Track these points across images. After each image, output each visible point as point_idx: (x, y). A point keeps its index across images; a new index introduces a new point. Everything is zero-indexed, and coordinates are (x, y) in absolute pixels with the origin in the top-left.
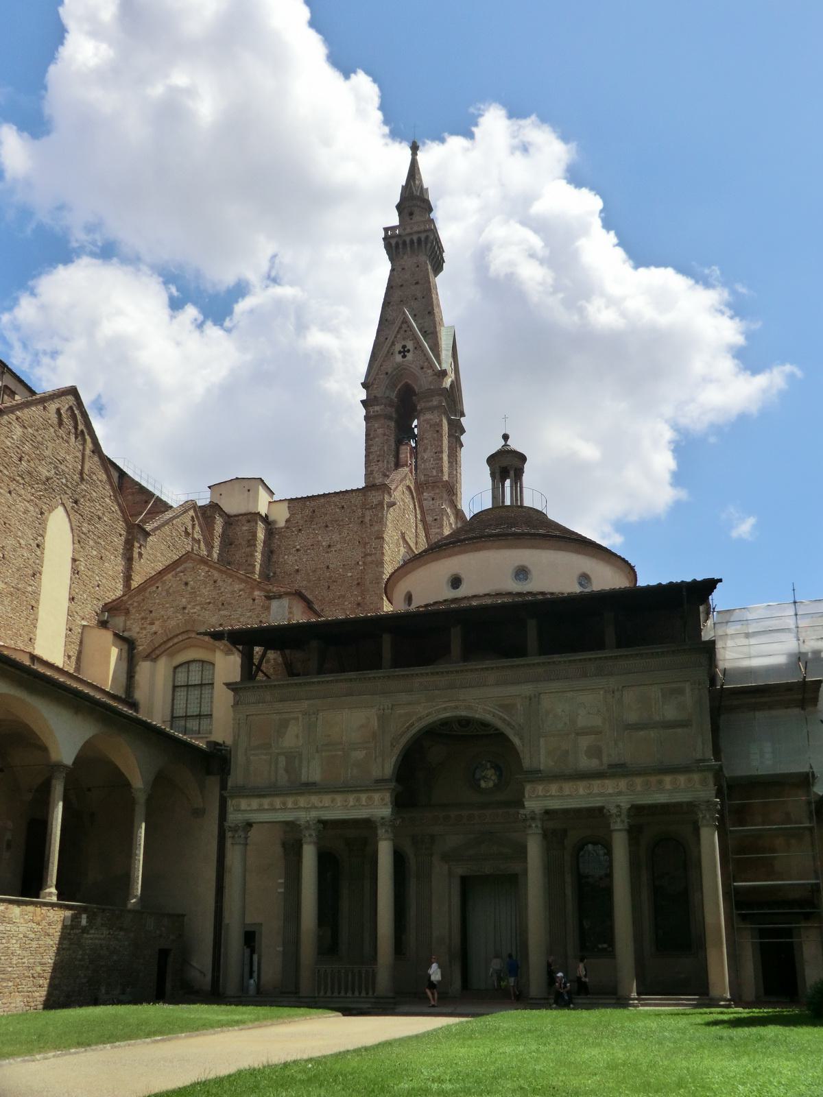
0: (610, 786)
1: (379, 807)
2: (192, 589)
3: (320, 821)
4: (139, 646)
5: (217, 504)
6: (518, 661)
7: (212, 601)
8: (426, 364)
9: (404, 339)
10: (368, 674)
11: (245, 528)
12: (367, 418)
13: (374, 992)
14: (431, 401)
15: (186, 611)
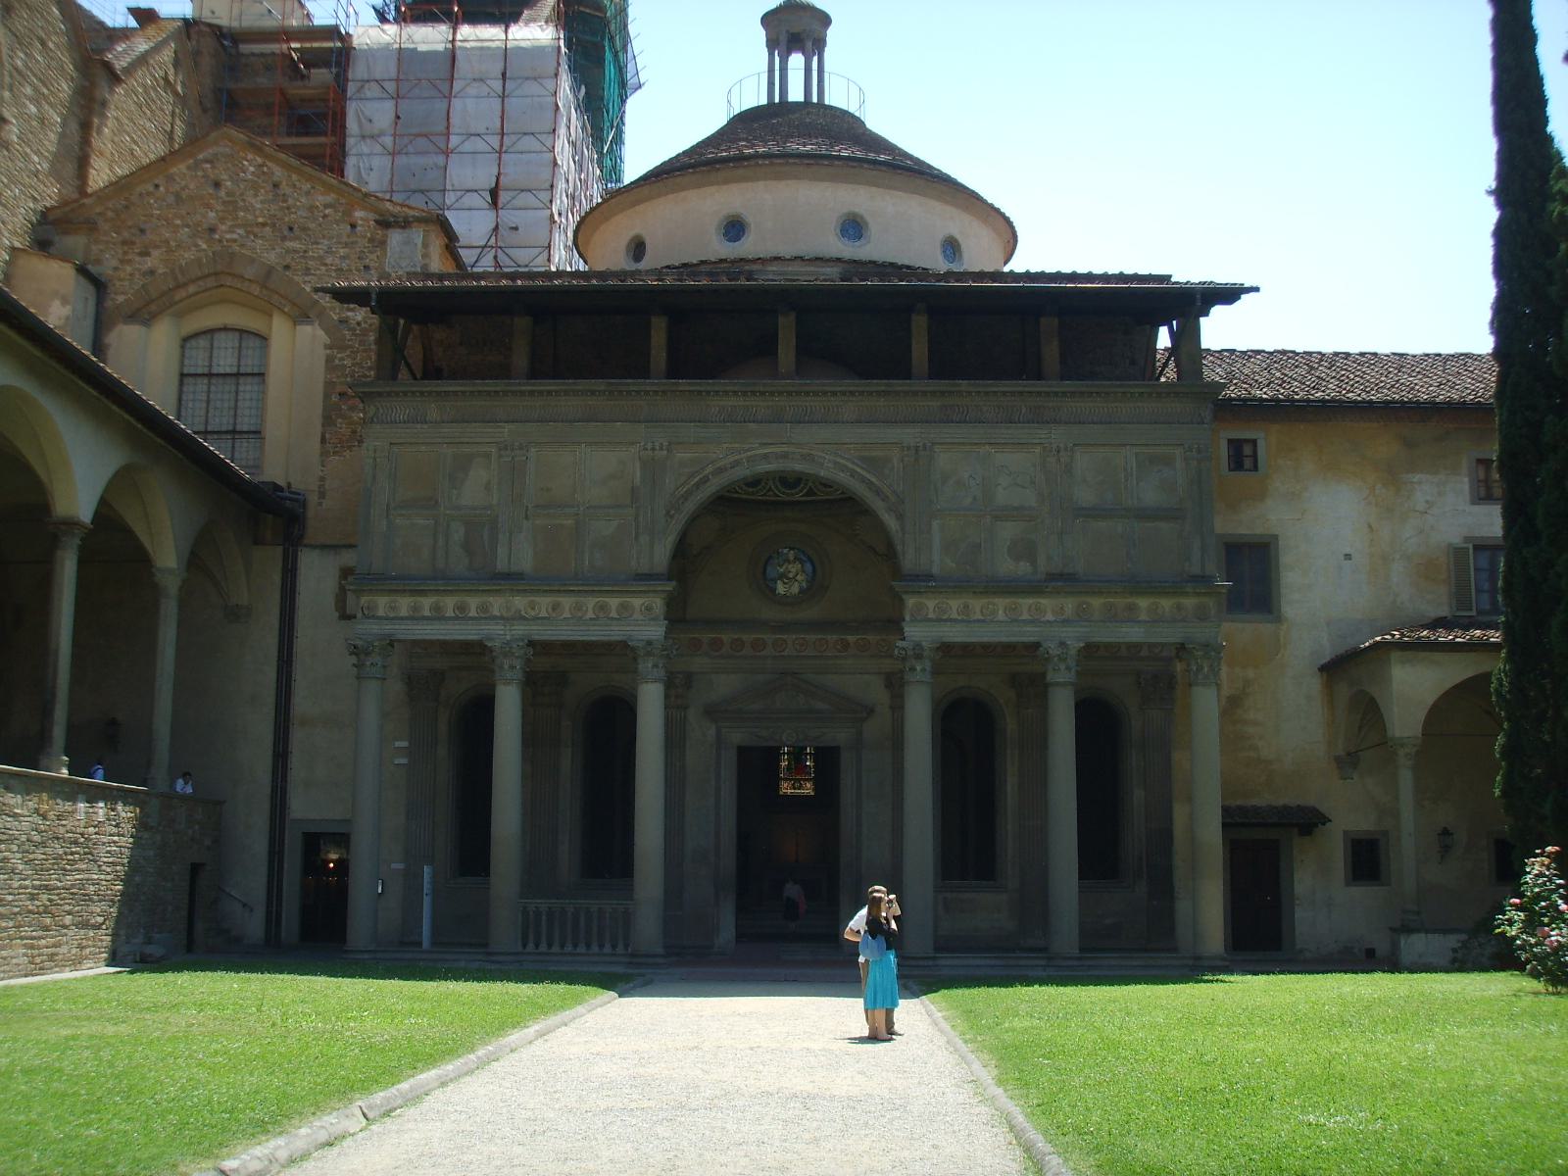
2: (228, 195)
3: (531, 643)
4: (116, 294)
6: (898, 385)
7: (269, 222)
10: (628, 384)
13: (626, 946)
15: (217, 237)
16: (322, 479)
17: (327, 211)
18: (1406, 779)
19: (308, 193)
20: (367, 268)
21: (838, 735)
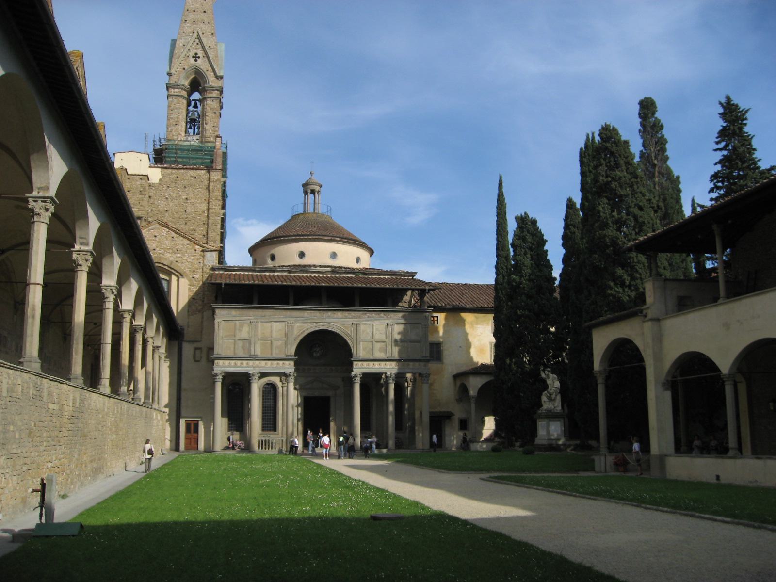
1: (289, 367)
5: (126, 169)
8: (210, 68)
9: (196, 49)
14: (212, 93)
15: (156, 251)
16: (188, 322)
17: (188, 246)
18: (473, 406)
19: (182, 240)
20: (200, 262)
21: (330, 393)
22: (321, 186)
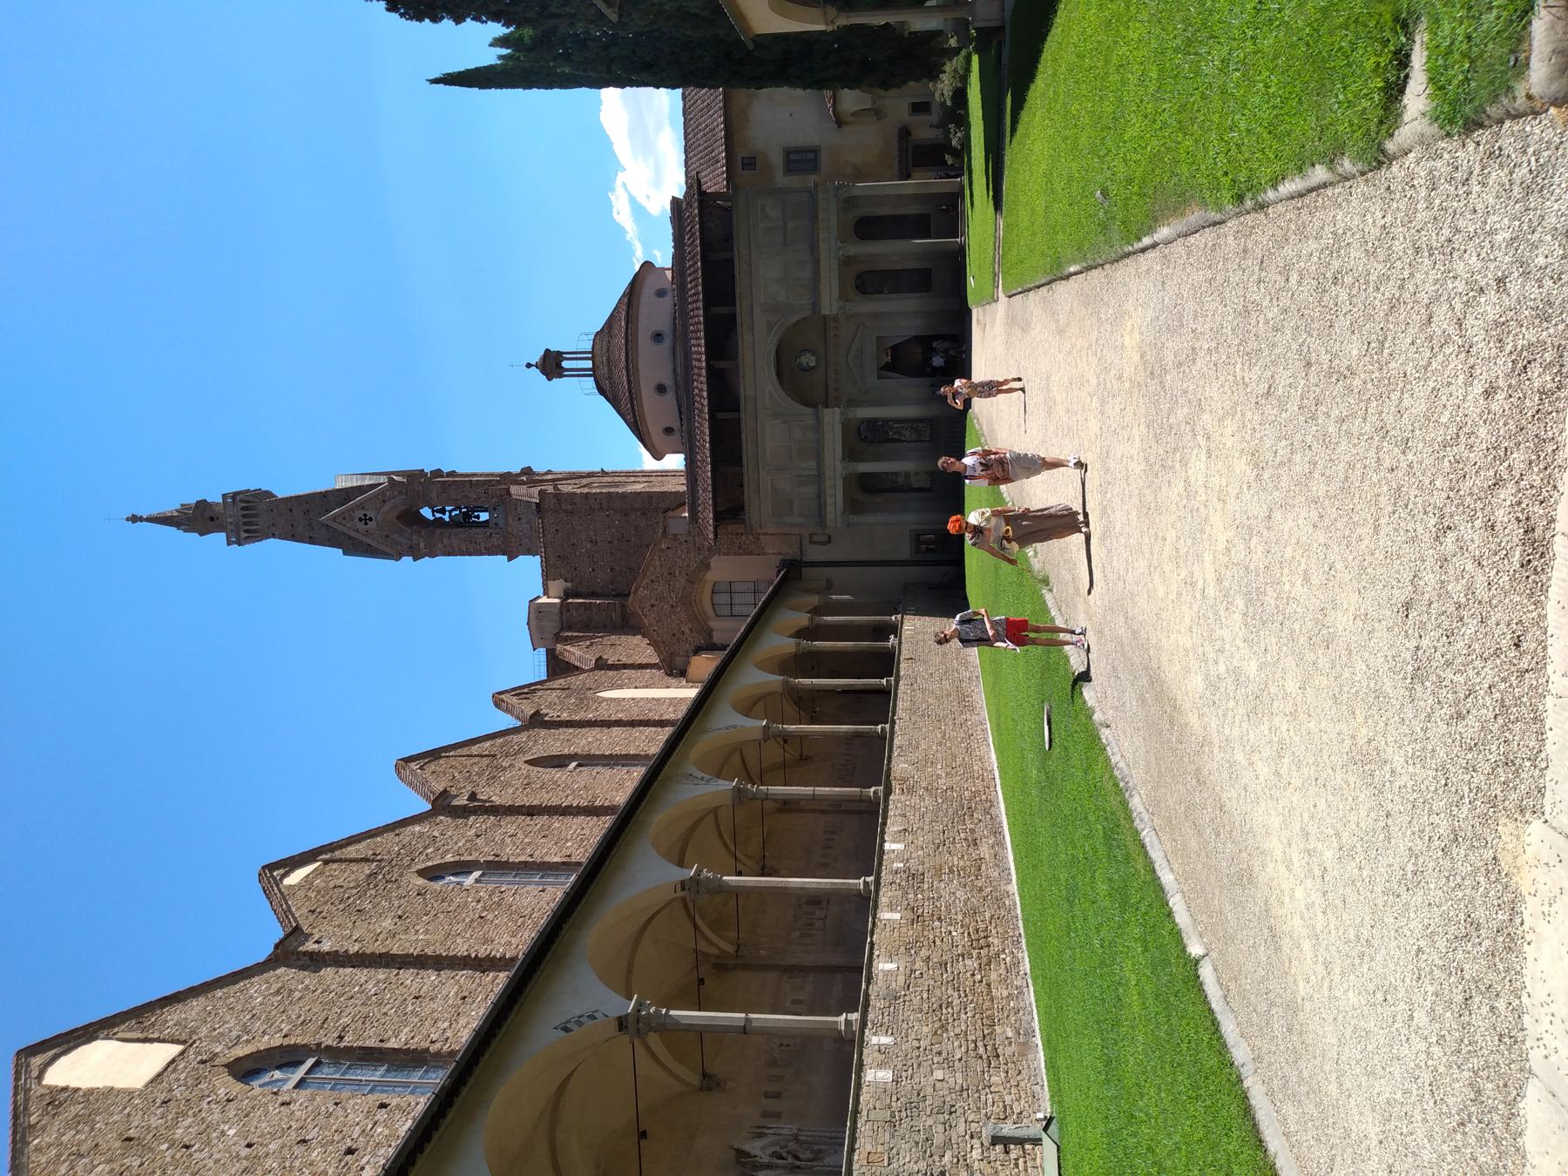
0: (823, 256)
9: (352, 520)
11: (574, 614)
12: (433, 555)
22: (547, 351)
